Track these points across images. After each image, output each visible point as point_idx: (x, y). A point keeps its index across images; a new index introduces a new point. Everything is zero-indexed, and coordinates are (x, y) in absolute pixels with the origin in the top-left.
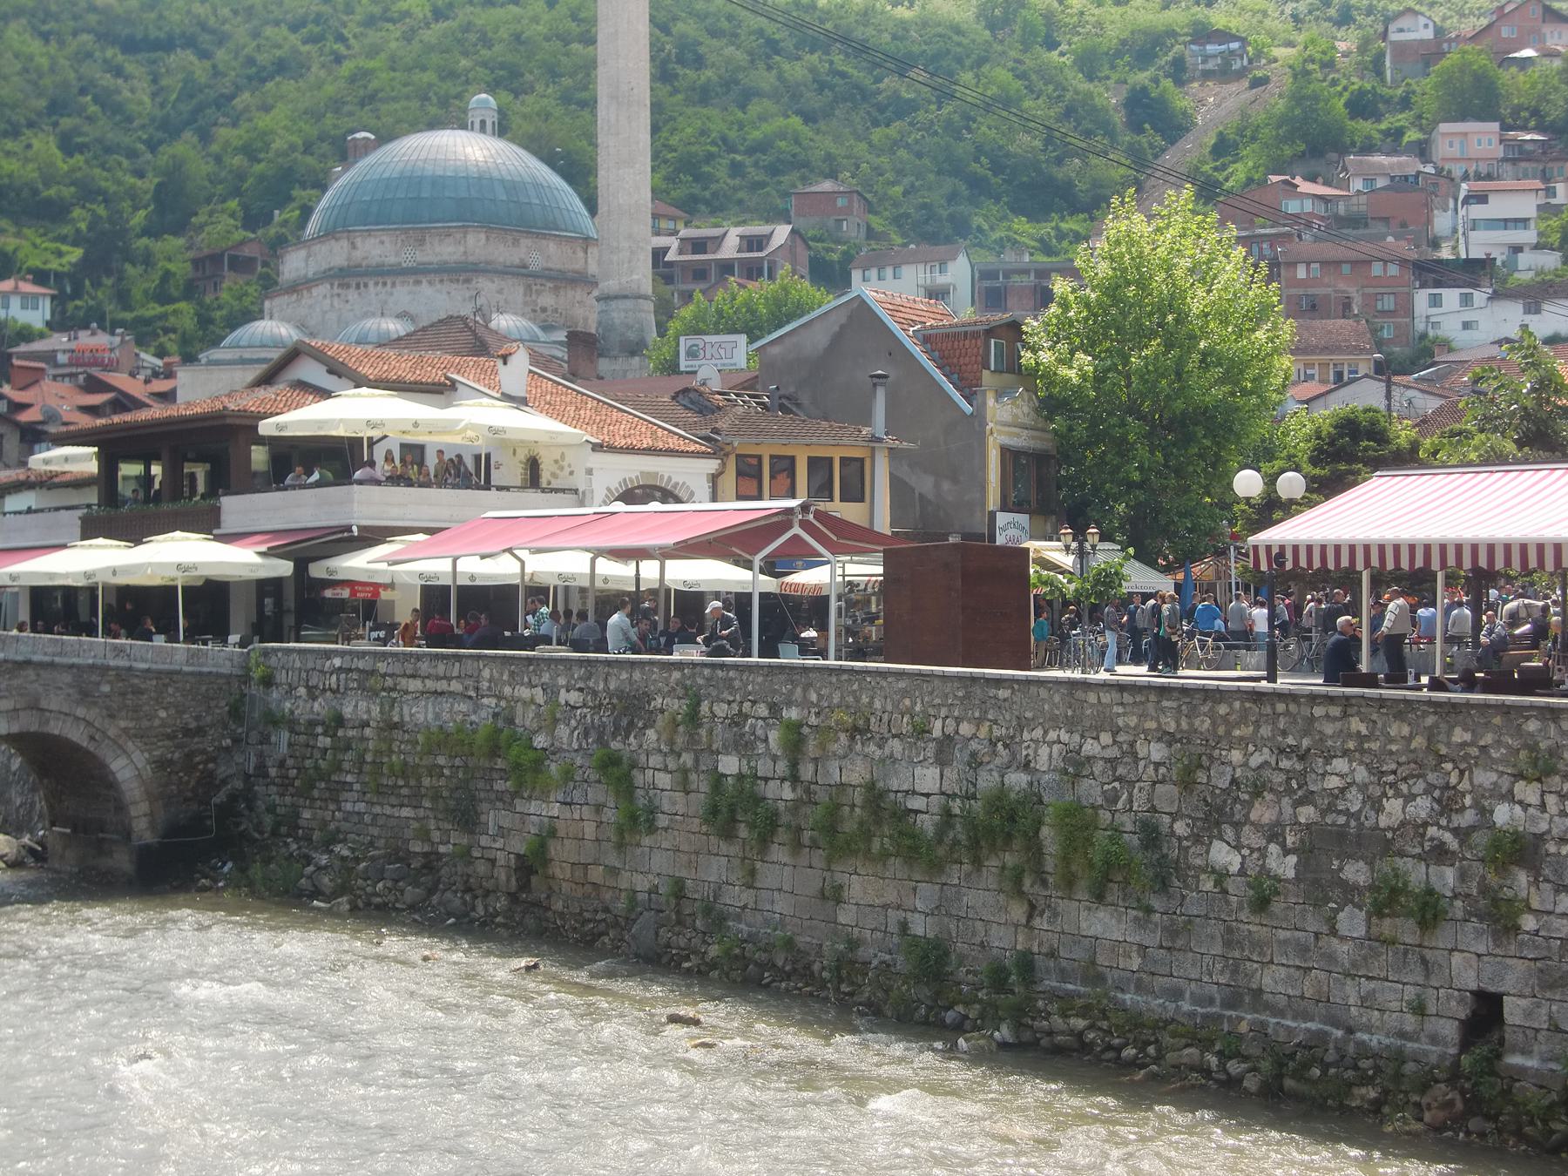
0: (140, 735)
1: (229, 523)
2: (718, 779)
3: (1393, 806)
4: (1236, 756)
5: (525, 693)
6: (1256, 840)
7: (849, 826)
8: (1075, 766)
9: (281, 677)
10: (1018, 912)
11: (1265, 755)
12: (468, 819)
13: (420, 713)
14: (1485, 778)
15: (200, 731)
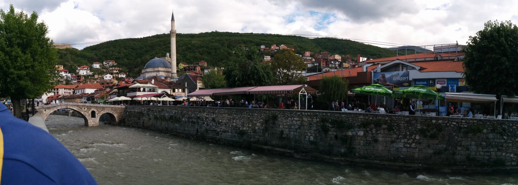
0: (116, 113)
1: (128, 96)
2: (155, 115)
3: (193, 115)
4: (184, 112)
5: (143, 109)
6: (185, 118)
7: (162, 118)
8: (175, 113)
9: (128, 108)
10: (172, 124)
11: (186, 112)
12: (139, 119)
13: (136, 111)
14: (197, 113)
15: (122, 113)
